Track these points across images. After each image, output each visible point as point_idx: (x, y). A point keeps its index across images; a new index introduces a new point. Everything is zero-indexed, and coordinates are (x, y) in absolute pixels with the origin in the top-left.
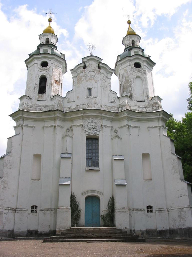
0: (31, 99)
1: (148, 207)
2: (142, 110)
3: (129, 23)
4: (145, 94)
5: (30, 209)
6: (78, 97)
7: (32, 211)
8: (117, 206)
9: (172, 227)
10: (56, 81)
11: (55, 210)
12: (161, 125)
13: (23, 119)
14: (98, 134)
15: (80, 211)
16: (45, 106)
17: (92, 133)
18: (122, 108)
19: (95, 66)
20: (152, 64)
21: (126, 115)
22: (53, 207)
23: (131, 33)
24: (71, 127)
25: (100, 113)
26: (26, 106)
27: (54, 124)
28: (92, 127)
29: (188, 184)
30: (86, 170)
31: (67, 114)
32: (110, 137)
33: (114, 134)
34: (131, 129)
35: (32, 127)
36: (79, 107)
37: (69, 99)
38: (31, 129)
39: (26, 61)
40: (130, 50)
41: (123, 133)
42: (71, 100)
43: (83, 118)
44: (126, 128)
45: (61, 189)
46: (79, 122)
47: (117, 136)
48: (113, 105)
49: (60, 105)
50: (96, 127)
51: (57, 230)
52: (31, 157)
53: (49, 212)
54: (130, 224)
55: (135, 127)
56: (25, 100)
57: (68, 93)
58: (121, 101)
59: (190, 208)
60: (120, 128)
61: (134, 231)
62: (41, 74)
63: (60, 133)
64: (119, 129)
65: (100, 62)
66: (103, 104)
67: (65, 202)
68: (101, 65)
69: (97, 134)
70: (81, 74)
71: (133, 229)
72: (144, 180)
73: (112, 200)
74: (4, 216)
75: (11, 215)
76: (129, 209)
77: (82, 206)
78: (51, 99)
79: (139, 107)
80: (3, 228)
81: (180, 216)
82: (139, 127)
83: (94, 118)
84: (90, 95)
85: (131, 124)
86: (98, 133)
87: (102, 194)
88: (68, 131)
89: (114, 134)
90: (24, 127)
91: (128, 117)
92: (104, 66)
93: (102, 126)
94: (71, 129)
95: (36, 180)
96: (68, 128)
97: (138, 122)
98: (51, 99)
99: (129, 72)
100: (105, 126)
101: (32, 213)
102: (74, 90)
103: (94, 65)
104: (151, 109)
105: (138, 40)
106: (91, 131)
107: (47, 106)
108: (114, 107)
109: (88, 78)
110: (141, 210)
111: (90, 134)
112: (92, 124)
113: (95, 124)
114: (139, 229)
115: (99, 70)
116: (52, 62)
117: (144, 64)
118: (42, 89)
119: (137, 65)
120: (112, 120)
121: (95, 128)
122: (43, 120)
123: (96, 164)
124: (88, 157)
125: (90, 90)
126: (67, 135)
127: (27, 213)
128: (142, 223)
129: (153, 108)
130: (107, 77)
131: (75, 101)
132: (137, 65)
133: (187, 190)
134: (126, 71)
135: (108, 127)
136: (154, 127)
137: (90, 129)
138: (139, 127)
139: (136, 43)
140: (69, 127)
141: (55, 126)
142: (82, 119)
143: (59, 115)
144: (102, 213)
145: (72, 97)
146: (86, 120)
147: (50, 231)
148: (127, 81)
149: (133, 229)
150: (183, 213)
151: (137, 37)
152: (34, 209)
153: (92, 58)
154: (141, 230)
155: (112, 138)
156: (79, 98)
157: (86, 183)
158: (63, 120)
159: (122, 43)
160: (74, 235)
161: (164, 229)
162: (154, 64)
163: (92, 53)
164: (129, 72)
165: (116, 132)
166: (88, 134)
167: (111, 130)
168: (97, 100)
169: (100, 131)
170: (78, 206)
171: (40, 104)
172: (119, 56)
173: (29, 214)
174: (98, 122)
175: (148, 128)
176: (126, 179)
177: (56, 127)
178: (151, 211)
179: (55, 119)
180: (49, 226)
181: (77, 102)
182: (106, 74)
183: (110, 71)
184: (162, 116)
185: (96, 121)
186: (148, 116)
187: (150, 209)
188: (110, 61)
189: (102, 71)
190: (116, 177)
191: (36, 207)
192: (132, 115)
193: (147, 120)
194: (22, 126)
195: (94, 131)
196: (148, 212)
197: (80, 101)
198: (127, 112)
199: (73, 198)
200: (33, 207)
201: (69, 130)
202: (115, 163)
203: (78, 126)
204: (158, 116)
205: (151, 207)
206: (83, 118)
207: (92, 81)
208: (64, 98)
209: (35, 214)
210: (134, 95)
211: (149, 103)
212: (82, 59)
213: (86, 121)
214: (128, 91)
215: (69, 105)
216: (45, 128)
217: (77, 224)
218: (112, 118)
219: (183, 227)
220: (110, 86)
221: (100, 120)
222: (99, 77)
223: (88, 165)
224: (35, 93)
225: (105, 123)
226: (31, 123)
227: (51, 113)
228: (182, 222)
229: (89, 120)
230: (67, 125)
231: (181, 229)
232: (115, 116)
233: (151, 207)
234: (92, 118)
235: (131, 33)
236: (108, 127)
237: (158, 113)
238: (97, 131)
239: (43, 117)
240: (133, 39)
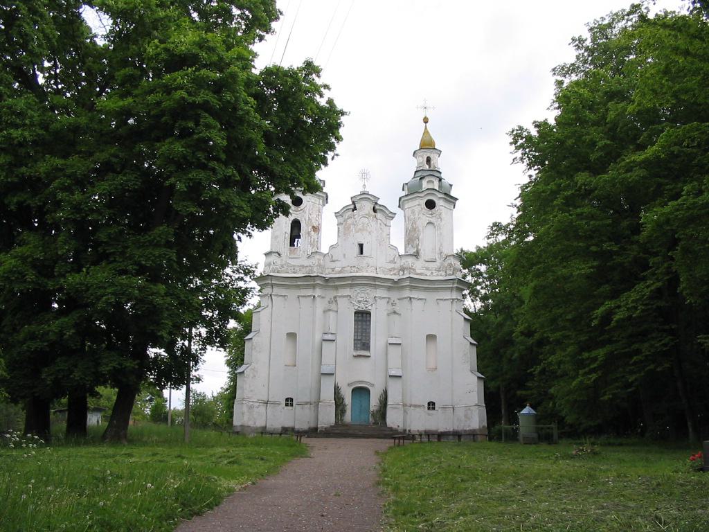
0: (279, 255)
1: (429, 404)
2: (432, 273)
3: (426, 121)
4: (437, 249)
5: (284, 403)
6: (344, 255)
7: (287, 405)
8: (390, 401)
9: (456, 428)
10: (313, 227)
11: (317, 403)
12: (454, 297)
13: (272, 285)
15: (345, 405)
16: (300, 266)
17: (362, 307)
18: (403, 271)
19: (369, 208)
20: (452, 200)
22: (313, 399)
23: (427, 144)
24: (335, 297)
25: (373, 282)
26: (274, 267)
27: (313, 292)
29: (479, 378)
30: (354, 356)
32: (385, 313)
33: (390, 308)
35: (285, 296)
36: (346, 269)
37: (332, 257)
41: (401, 307)
42: (334, 258)
45: (324, 380)
46: (347, 292)
47: (395, 312)
48: (392, 265)
49: (319, 265)
51: (319, 426)
52: (284, 337)
53: (308, 406)
54: (405, 421)
55: (420, 299)
56: (273, 258)
57: (332, 247)
58: (403, 261)
59: (477, 407)
61: (409, 431)
63: (320, 305)
65: (376, 203)
66: (379, 265)
67: (328, 395)
68: (377, 207)
70: (349, 221)
71: (408, 429)
72: (427, 368)
73: (385, 392)
74: (255, 410)
75: (262, 409)
76: (404, 405)
77: (348, 400)
79: (427, 269)
80: (255, 423)
81: (466, 416)
84: (362, 253)
85: (414, 294)
86: (370, 308)
87: (373, 385)
89: (390, 308)
90: (273, 296)
92: (381, 208)
95: (289, 366)
99: (417, 216)
100: (380, 297)
101: (286, 408)
102: (339, 244)
103: (368, 207)
104: (443, 273)
105: (436, 156)
107: (303, 266)
108: (394, 269)
109: (358, 227)
110: (419, 406)
111: (360, 309)
112: (363, 295)
114: (416, 429)
115: (374, 214)
117: (440, 203)
119: (430, 205)
120: (389, 288)
121: (366, 301)
122: (298, 287)
123: (366, 346)
124: (356, 338)
125: (361, 246)
126: (330, 310)
127: (280, 406)
128: (419, 422)
129: (446, 272)
130: (386, 225)
132: (430, 205)
133: (476, 384)
134: (413, 212)
135: (383, 298)
137: (359, 302)
139: (432, 162)
141: (314, 297)
143: (318, 282)
144: (371, 409)
145: (337, 254)
147: (309, 428)
148: (414, 229)
149: (408, 429)
150: (469, 412)
151: (434, 151)
152: (289, 402)
153: (365, 196)
154: (418, 431)
156: (346, 256)
157: (351, 372)
158: (324, 287)
159: (414, 155)
160: (338, 431)
161: (446, 430)
162: (456, 199)
163: (364, 185)
164: (417, 216)
165: (393, 305)
167: (388, 302)
168: (370, 261)
170: (343, 399)
171: (294, 264)
172: (407, 184)
173: (283, 408)
176: (403, 367)
178: (434, 409)
179: (314, 287)
180: (308, 422)
181: (344, 263)
182: (384, 219)
183: (390, 215)
184: (456, 285)
185: (368, 291)
187: (431, 405)
188: (389, 200)
189: (379, 215)
190: (389, 366)
191: (292, 400)
192: (416, 283)
194: (271, 295)
196: (429, 408)
197: (347, 264)
199: (337, 390)
200: (287, 400)
202: (389, 347)
203: (344, 296)
204: (451, 286)
205: (433, 404)
206: (351, 286)
207: (364, 233)
208: (325, 255)
209: (291, 408)
210: (422, 252)
211: (442, 264)
214: (415, 245)
215: (333, 265)
216: (300, 298)
217: (342, 420)
219: (468, 429)
220: (389, 238)
222: (373, 225)
223: (356, 348)
224: (284, 247)
225: (380, 293)
226: (283, 292)
227: (310, 281)
228: (468, 422)
230: (331, 294)
231: (465, 431)
232: (395, 285)
233: (433, 404)
235: (427, 144)
237: (452, 281)
240: (429, 155)
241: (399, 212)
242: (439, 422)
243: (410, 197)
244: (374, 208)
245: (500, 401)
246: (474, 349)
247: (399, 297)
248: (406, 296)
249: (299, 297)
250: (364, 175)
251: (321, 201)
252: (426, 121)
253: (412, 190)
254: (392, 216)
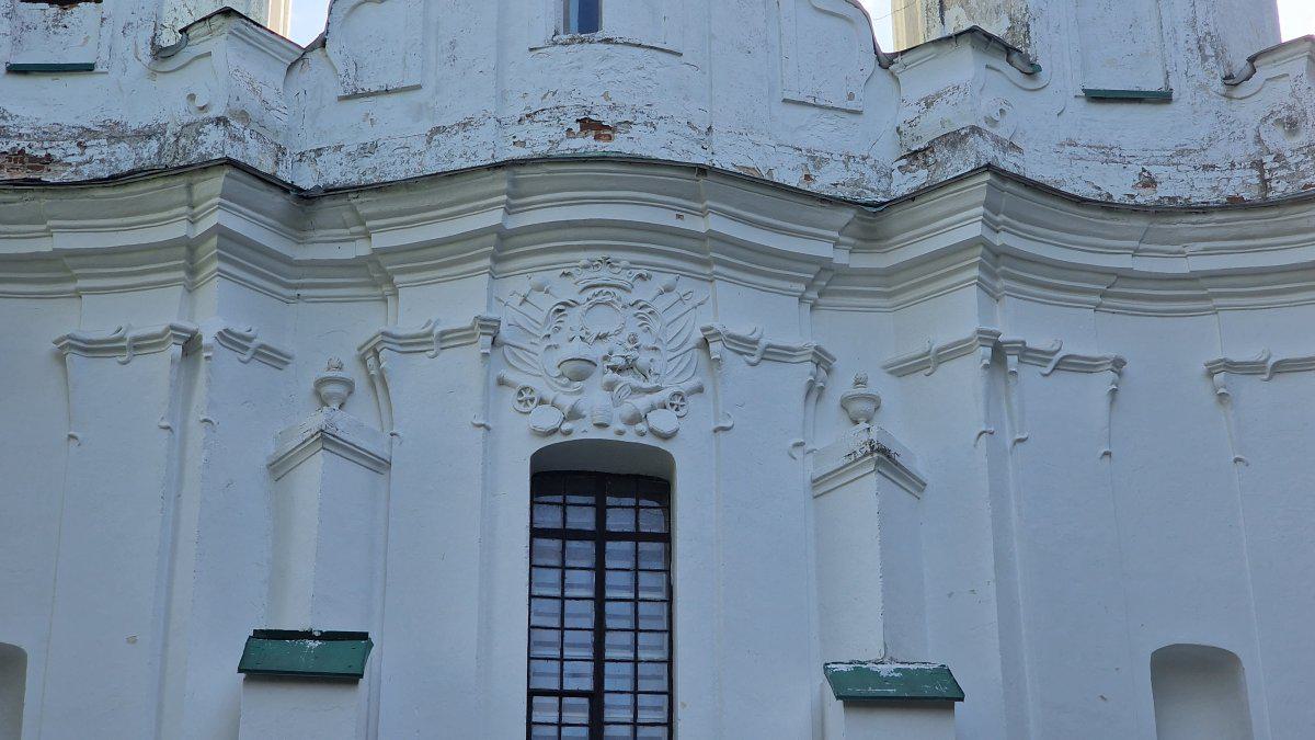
14: (666, 428)
17: (601, 416)
21: (975, 230)
28: (600, 350)
31: (329, 210)
34: (1030, 374)
43: (497, 260)
44: (970, 371)
50: (643, 359)
55: (1067, 364)
60: (902, 370)
64: (893, 380)
69: (652, 431)
78: (161, 53)
79: (1108, 154)
82: (1118, 364)
83: (624, 258)
86: (664, 421)
91: (997, 254)
93: (715, 347)
94: (373, 385)
96: (340, 368)
97: (1097, 308)
100: (742, 345)
111: (583, 431)
113: (633, 327)
121: (629, 366)
131: (418, 87)
135: (777, 354)
136: (1281, 368)
138: (1118, 364)
140: (349, 357)
141: (192, 345)
142: (487, 262)
146: (537, 278)
155: (816, 482)
166: (554, 431)
167: (814, 391)
169: (691, 400)
174: (673, 297)
175: (1210, 374)
177: (209, 348)
185: (644, 292)
186: (1207, 252)
193: (1197, 290)
195: (617, 402)
198: (982, 197)
201: (349, 385)
208: (299, 58)
213: (540, 289)
216: (74, 359)
218: (825, 267)
221: (684, 286)
225: (737, 308)
229: (570, 280)
234: (599, 255)
236: (777, 354)
238: (656, 398)
247: (891, 356)
248: (942, 339)
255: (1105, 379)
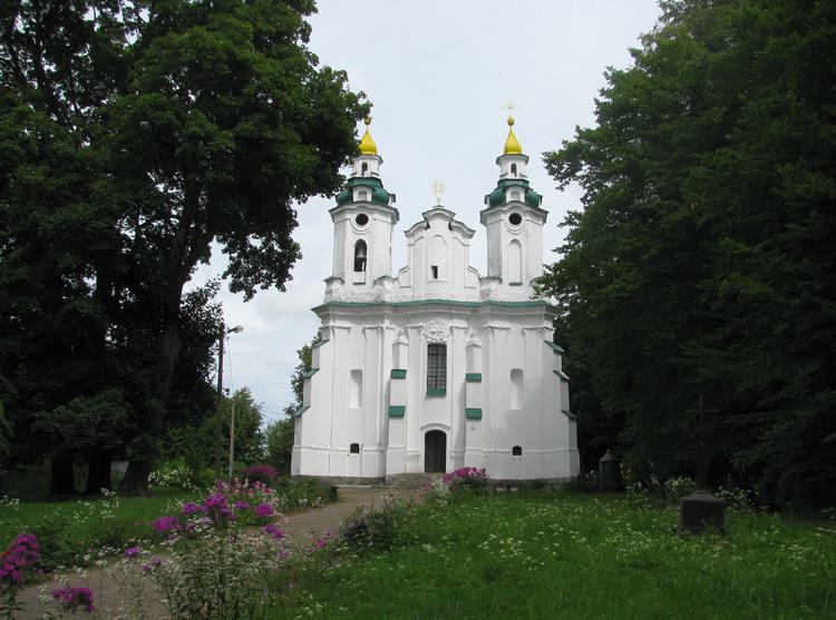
3: (511, 123)
17: (436, 339)
38: (345, 331)
39: (330, 211)
40: (504, 191)
55: (503, 329)
62: (358, 238)
68: (453, 224)
84: (436, 276)
88: (399, 335)
98: (375, 283)
105: (523, 163)
106: (435, 336)
111: (434, 341)
116: (376, 216)
118: (359, 265)
119: (515, 219)
120: (467, 318)
125: (435, 269)
137: (433, 333)
153: (439, 212)
162: (546, 213)
189: (456, 234)
196: (514, 454)
212: (423, 214)
239: (365, 313)
241: (481, 230)
242: (524, 471)
243: (493, 211)
244: (450, 225)
245: (589, 444)
246: (566, 385)
249: (365, 328)
250: (438, 188)
251: (389, 220)
252: (511, 123)
253: (496, 201)
254: (470, 234)
255: (504, 332)
